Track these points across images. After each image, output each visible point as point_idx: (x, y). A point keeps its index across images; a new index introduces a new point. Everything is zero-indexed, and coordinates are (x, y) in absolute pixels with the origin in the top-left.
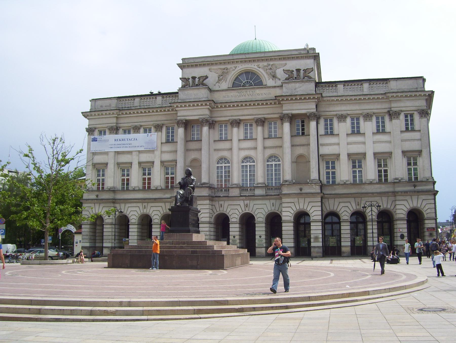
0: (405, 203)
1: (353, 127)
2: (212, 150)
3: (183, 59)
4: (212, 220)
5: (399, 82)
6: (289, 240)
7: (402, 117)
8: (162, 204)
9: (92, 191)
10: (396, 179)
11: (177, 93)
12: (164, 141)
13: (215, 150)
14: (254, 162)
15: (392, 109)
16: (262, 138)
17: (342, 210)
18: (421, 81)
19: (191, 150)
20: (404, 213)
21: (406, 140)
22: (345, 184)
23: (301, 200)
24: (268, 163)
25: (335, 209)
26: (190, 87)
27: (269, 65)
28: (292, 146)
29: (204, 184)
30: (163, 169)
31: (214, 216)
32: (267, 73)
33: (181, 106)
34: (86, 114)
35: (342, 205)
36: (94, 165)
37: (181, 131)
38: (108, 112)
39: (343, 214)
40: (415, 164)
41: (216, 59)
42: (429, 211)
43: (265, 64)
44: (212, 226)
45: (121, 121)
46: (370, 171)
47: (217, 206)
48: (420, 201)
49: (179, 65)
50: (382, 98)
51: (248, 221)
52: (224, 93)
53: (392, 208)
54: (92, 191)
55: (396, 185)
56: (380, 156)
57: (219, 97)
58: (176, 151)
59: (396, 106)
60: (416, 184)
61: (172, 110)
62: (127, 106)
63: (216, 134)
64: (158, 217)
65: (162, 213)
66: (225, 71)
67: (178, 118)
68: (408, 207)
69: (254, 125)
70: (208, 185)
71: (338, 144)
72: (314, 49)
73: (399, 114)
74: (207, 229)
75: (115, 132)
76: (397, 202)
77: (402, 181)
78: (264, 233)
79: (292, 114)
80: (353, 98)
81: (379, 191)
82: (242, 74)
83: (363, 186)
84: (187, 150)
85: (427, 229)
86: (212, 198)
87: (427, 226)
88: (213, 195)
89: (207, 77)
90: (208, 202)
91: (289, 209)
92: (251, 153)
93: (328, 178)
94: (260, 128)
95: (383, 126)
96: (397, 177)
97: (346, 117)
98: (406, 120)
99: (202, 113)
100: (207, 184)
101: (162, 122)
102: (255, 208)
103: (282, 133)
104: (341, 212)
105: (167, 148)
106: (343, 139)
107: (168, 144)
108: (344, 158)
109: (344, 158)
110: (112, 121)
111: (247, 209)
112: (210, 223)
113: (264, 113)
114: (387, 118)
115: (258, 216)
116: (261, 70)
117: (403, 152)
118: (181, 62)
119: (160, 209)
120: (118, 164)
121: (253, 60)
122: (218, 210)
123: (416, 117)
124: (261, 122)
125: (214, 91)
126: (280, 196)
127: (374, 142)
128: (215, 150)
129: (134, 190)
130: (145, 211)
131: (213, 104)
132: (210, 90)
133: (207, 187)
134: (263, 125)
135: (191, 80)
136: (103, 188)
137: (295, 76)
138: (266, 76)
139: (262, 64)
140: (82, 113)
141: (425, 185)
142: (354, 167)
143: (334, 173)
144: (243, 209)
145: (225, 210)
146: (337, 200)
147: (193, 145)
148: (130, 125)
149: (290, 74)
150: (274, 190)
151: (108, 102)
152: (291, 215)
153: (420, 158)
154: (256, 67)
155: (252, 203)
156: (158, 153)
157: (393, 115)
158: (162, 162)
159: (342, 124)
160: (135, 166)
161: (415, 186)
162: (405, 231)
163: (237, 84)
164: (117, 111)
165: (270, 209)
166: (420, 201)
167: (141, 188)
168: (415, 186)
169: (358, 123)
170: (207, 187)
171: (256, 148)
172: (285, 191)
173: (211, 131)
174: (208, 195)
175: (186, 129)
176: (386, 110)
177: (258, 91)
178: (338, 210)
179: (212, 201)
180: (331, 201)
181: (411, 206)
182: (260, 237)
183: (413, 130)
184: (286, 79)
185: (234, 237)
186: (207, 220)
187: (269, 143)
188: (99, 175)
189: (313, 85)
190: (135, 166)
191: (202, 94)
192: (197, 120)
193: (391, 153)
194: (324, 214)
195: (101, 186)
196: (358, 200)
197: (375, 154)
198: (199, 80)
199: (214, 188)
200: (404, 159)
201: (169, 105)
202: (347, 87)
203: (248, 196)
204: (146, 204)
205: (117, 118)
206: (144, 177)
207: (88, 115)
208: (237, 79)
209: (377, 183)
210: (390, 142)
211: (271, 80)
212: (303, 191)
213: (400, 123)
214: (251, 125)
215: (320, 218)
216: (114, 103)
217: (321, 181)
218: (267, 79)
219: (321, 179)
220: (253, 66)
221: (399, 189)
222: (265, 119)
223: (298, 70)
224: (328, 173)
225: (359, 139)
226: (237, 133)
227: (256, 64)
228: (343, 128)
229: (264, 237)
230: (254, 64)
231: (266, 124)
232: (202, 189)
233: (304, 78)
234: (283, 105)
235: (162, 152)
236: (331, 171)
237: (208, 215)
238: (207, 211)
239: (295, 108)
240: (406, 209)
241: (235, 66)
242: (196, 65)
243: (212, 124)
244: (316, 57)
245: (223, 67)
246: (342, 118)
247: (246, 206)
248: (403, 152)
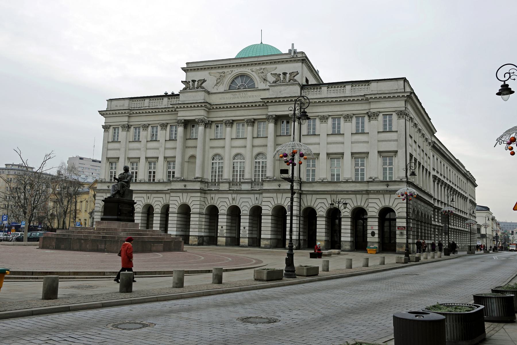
0: (377, 201)
1: (334, 128)
2: (207, 147)
3: (187, 63)
4: (204, 211)
5: (380, 84)
6: (267, 233)
7: (381, 117)
8: (163, 196)
9: (105, 182)
10: (371, 178)
11: (178, 95)
12: (168, 139)
13: (211, 147)
14: (244, 159)
15: (371, 110)
16: (251, 138)
17: (319, 206)
18: (402, 82)
19: (189, 147)
20: (376, 211)
21: (383, 141)
22: (322, 182)
23: (280, 195)
24: (256, 161)
25: (312, 205)
26: (190, 89)
27: (261, 69)
28: (277, 145)
29: (197, 178)
30: (166, 163)
32: (259, 77)
33: (181, 107)
34: (102, 113)
35: (319, 201)
36: (108, 159)
37: (180, 129)
38: (120, 112)
39: (320, 210)
40: (391, 164)
41: (215, 63)
42: (400, 210)
43: (258, 67)
45: (132, 119)
47: (209, 198)
48: (392, 200)
49: (183, 69)
50: (362, 99)
51: (235, 213)
52: (220, 95)
53: (365, 206)
54: (105, 182)
55: (370, 184)
56: (357, 155)
57: (215, 100)
58: (176, 148)
59: (375, 107)
60: (389, 183)
61: (175, 111)
62: (138, 106)
63: (211, 132)
64: (159, 207)
65: (163, 203)
66: (222, 74)
67: (179, 118)
68: (381, 206)
69: (246, 125)
70: (200, 180)
71: (319, 144)
72: (303, 53)
73: (378, 116)
75: (126, 129)
76: (370, 201)
77: (376, 180)
78: (248, 224)
79: (276, 115)
80: (334, 100)
81: (353, 189)
82: (238, 77)
83: (339, 184)
84: (185, 147)
85: (398, 228)
86: (202, 191)
87: (398, 225)
88: (206, 188)
89: (204, 81)
90: (199, 194)
91: (269, 204)
93: (308, 175)
94: (250, 128)
95: (363, 127)
96: (371, 176)
97: (327, 119)
98: (385, 121)
99: (199, 114)
100: (200, 178)
101: (167, 122)
102: (241, 201)
103: (267, 134)
104: (317, 208)
105: (170, 144)
106: (323, 139)
107: (171, 142)
108: (323, 156)
109: (323, 156)
110: (124, 120)
112: (200, 214)
113: (254, 114)
114: (366, 118)
115: (243, 209)
116: (253, 73)
117: (379, 152)
118: (185, 66)
119: (161, 199)
120: (129, 159)
121: (248, 65)
122: (209, 202)
124: (252, 122)
125: (212, 93)
126: (261, 192)
128: (211, 147)
129: (140, 183)
130: (149, 202)
131: (208, 105)
132: (209, 93)
133: (199, 181)
134: (253, 126)
135: (191, 83)
136: (136, 180)
137: (282, 79)
138: (258, 79)
139: (255, 68)
140: (99, 111)
141: (398, 185)
143: (314, 171)
145: (215, 203)
146: (315, 197)
147: (190, 143)
148: (139, 123)
149: (277, 77)
150: (257, 186)
151: (122, 102)
152: (270, 209)
153: (396, 158)
154: (250, 71)
155: (239, 196)
156: (162, 149)
157: (372, 116)
158: (165, 158)
159: (324, 125)
160: (143, 160)
161: (388, 186)
162: (376, 229)
163: (232, 88)
164: (128, 111)
165: (254, 203)
166: (392, 200)
167: (147, 180)
168: (388, 186)
169: (339, 124)
170: (199, 181)
171: (245, 147)
172: (266, 186)
173: (208, 130)
174: (199, 188)
175: (185, 127)
176: (365, 112)
177: (249, 94)
178: (315, 206)
179: (205, 193)
180: (309, 197)
181: (384, 205)
184: (273, 82)
185: (222, 227)
186: (198, 211)
187: (257, 142)
188: (112, 168)
189: (298, 88)
190: (143, 160)
191: (199, 97)
192: (194, 120)
193: (368, 153)
194: (302, 209)
195: (152, 178)
196: (334, 197)
197: (352, 154)
198: (198, 83)
199: (207, 183)
200: (379, 158)
201: (171, 106)
202: (330, 89)
203: (237, 190)
204: (149, 195)
205: (129, 117)
206: (150, 170)
207: (104, 114)
208: (233, 81)
209: (353, 182)
210: (368, 142)
211: (262, 83)
212: (282, 188)
213: (378, 123)
214: (243, 125)
216: (126, 104)
217: (300, 178)
218: (259, 82)
219: (302, 176)
220: (247, 70)
221: (372, 187)
222: (255, 119)
223: (285, 74)
224: (308, 171)
225: (338, 139)
226: (229, 132)
227: (250, 68)
228: (324, 128)
230: (247, 68)
231: (256, 125)
232: (195, 183)
233: (289, 81)
234: (269, 107)
235: (165, 149)
236: (311, 169)
237: (198, 206)
238: (198, 203)
239: (278, 110)
240: (378, 208)
241: (232, 70)
242: (198, 69)
243: (208, 124)
244: (305, 60)
245: (221, 71)
246: (324, 119)
247: (233, 199)
248: (379, 152)
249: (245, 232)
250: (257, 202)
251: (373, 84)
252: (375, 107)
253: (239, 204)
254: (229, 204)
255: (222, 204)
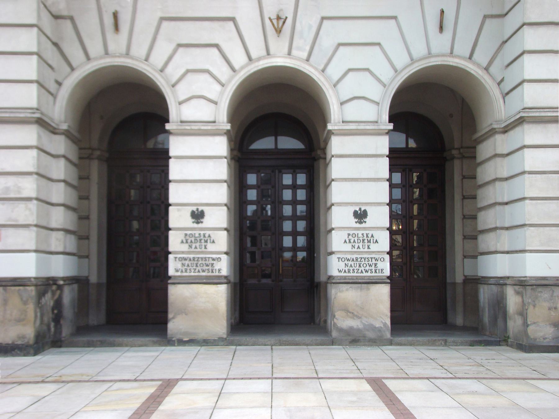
4: (59, 111)
31: (72, 81)
44: (60, 145)
74: (27, 160)
102: (327, 42)
111: (279, 46)
115: (348, 88)
122: (95, 47)
144: (257, 50)
145: (139, 49)
165: (419, 50)
182: (361, 216)
185: (198, 216)
229: (380, 217)
249: (370, 240)
250: (440, 43)
253: (319, 59)
254: (238, 58)
255: (185, 60)
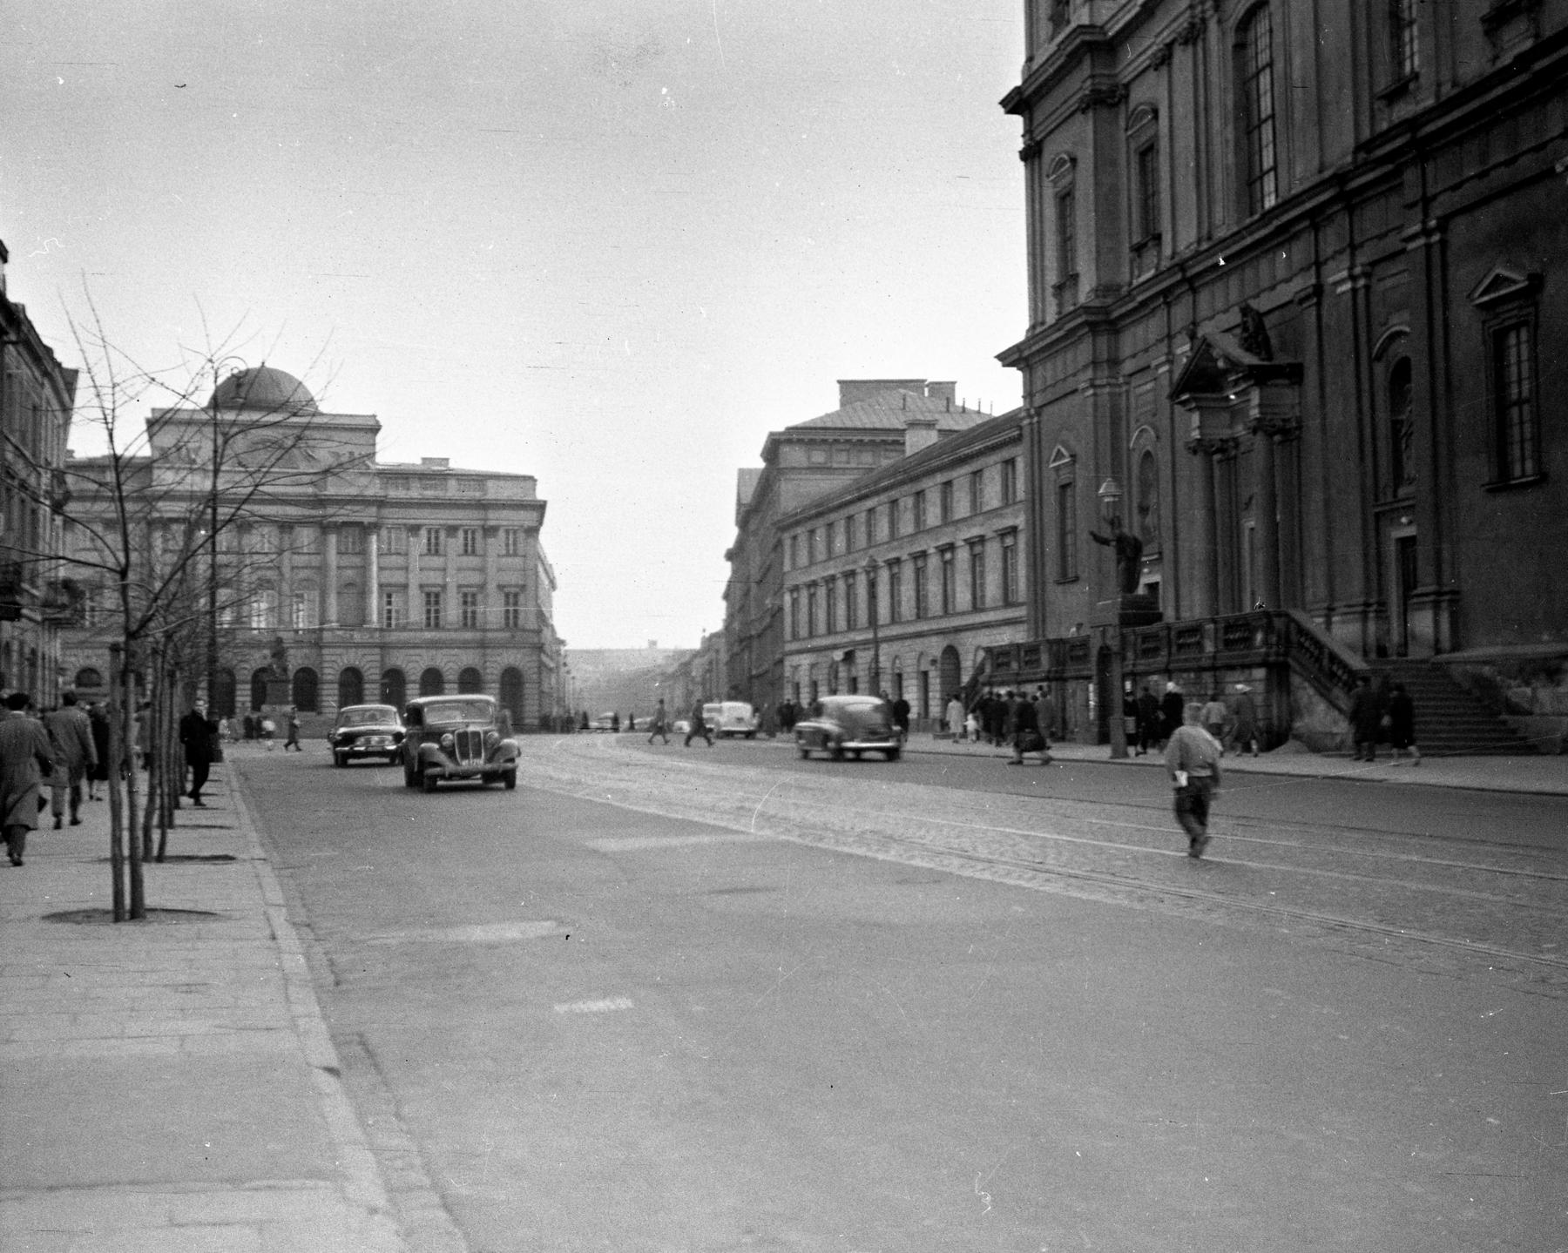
1: (429, 544)
46: (452, 610)
59: (494, 517)
92: (270, 574)
109: (414, 591)
123: (521, 536)
127: (459, 570)
142: (428, 603)
183: (515, 555)
215: (377, 677)
251: (490, 483)
252: (494, 517)
